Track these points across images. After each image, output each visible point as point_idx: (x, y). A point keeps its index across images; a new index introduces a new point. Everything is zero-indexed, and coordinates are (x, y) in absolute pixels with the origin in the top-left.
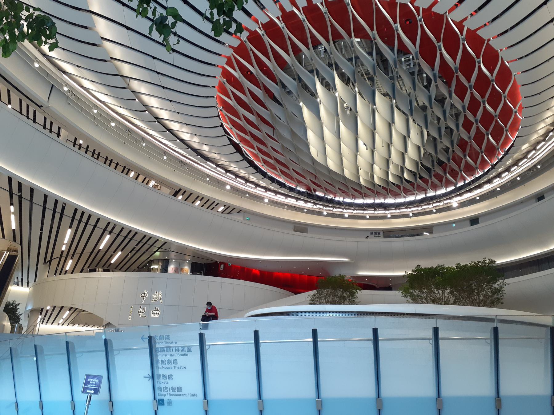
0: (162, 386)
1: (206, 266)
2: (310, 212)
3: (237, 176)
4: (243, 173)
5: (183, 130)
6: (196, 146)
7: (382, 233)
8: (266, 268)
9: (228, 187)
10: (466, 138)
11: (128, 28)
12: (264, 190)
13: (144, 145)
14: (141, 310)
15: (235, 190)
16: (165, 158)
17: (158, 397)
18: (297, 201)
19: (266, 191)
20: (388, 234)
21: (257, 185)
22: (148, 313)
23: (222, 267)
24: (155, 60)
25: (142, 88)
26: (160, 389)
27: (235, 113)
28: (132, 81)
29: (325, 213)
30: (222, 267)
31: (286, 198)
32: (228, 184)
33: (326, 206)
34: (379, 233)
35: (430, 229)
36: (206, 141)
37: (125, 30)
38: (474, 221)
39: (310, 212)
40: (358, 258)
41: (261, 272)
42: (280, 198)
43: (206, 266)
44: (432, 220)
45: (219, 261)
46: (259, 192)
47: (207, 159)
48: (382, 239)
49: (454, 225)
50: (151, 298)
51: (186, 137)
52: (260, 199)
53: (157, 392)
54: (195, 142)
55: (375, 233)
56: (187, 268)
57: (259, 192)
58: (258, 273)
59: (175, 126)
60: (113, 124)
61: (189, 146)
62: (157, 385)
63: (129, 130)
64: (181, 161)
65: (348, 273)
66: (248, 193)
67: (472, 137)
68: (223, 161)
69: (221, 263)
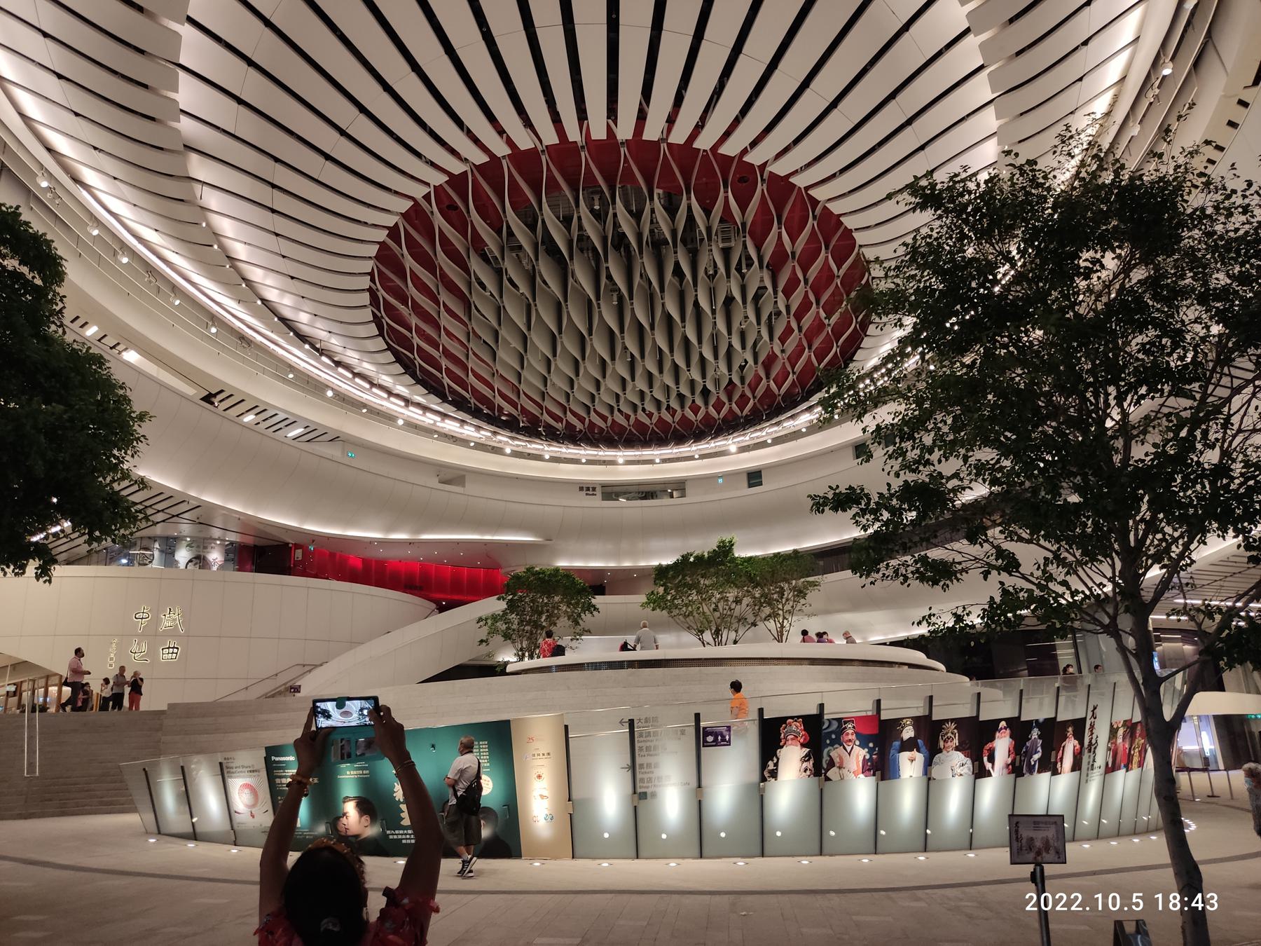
0: (645, 776)
1: (266, 554)
2: (480, 447)
3: (390, 393)
4: (386, 380)
5: (268, 282)
6: (288, 314)
7: (599, 492)
8: (382, 553)
9: (330, 394)
10: (778, 352)
11: (240, 101)
12: (402, 404)
13: (177, 302)
14: (134, 648)
15: (343, 399)
16: (214, 330)
17: (639, 790)
18: (443, 420)
19: (407, 406)
20: (611, 492)
21: (408, 402)
22: (152, 652)
23: (299, 554)
24: (278, 165)
25: (212, 200)
26: (642, 780)
27: (400, 271)
28: (198, 187)
29: (508, 451)
30: (299, 554)
31: (443, 420)
32: (328, 386)
33: (512, 438)
34: (594, 489)
35: (680, 486)
36: (308, 305)
37: (234, 104)
38: (754, 477)
39: (480, 447)
40: (555, 533)
41: (366, 562)
42: (429, 419)
43: (266, 554)
44: (687, 469)
45: (291, 541)
46: (395, 406)
47: (302, 338)
48: (597, 501)
49: (720, 481)
50: (157, 621)
51: (272, 295)
52: (389, 418)
53: (638, 785)
54: (285, 302)
55: (587, 489)
56: (215, 557)
57: (395, 406)
58: (361, 566)
59: (256, 275)
60: (125, 260)
61: (275, 312)
62: (639, 776)
63: (150, 269)
64: (242, 338)
65: (542, 563)
66: (364, 406)
67: (788, 352)
68: (335, 343)
69: (297, 546)
